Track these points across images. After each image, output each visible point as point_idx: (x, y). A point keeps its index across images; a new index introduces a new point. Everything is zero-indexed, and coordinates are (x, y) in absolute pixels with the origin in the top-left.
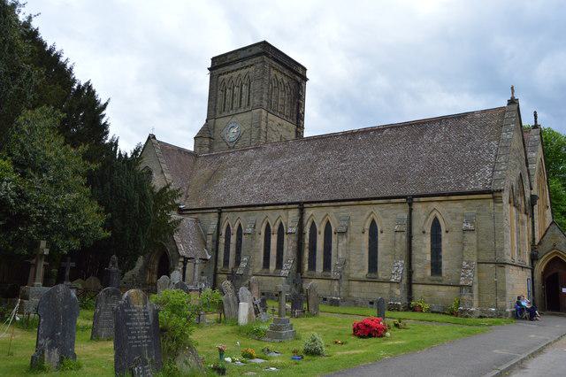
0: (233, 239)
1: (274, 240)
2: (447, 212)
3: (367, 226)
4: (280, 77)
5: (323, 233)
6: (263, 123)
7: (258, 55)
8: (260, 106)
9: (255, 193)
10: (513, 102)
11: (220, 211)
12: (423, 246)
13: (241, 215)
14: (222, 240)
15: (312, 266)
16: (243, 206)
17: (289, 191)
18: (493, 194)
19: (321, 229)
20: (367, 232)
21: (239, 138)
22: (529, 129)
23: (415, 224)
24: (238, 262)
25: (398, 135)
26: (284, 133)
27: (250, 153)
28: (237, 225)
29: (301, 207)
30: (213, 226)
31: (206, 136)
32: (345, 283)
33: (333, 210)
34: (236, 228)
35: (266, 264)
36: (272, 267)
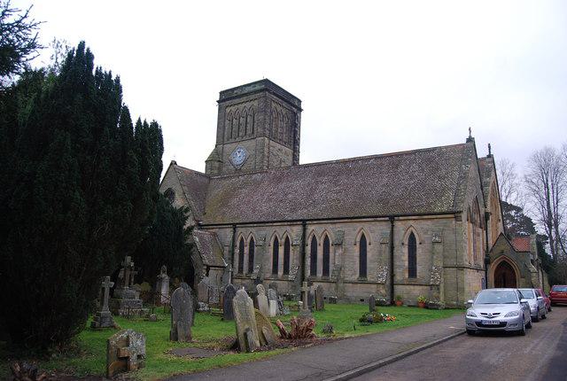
0: (246, 250)
1: (281, 250)
2: (421, 228)
3: (358, 239)
4: (279, 108)
5: (322, 245)
6: (266, 149)
7: (261, 90)
8: (264, 135)
9: (264, 209)
10: (470, 140)
11: (234, 226)
12: (403, 254)
13: (253, 230)
14: (237, 251)
15: (314, 272)
16: (255, 223)
17: (293, 210)
18: (456, 215)
19: (320, 241)
20: (358, 244)
21: (245, 162)
22: (483, 159)
23: (396, 237)
24: (251, 270)
25: (382, 164)
26: (283, 157)
27: (258, 177)
28: (249, 238)
29: (304, 223)
30: (230, 239)
31: (215, 160)
32: (341, 285)
33: (331, 226)
34: (249, 240)
35: (275, 270)
36: (280, 273)
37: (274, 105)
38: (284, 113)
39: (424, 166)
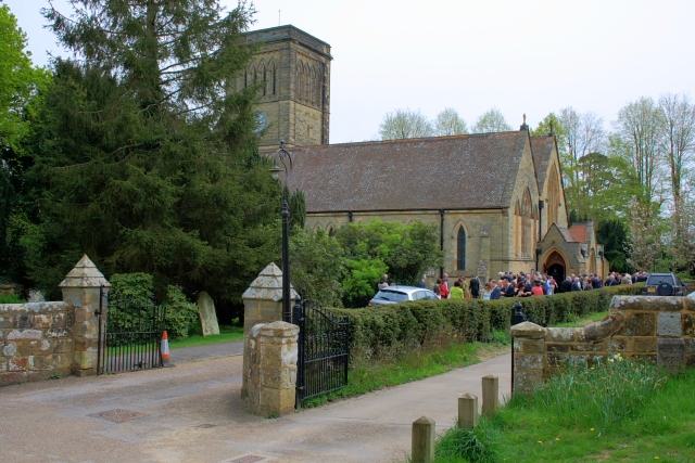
2: (470, 222)
6: (292, 116)
26: (311, 122)
37: (299, 57)
38: (304, 62)
39: (476, 154)
